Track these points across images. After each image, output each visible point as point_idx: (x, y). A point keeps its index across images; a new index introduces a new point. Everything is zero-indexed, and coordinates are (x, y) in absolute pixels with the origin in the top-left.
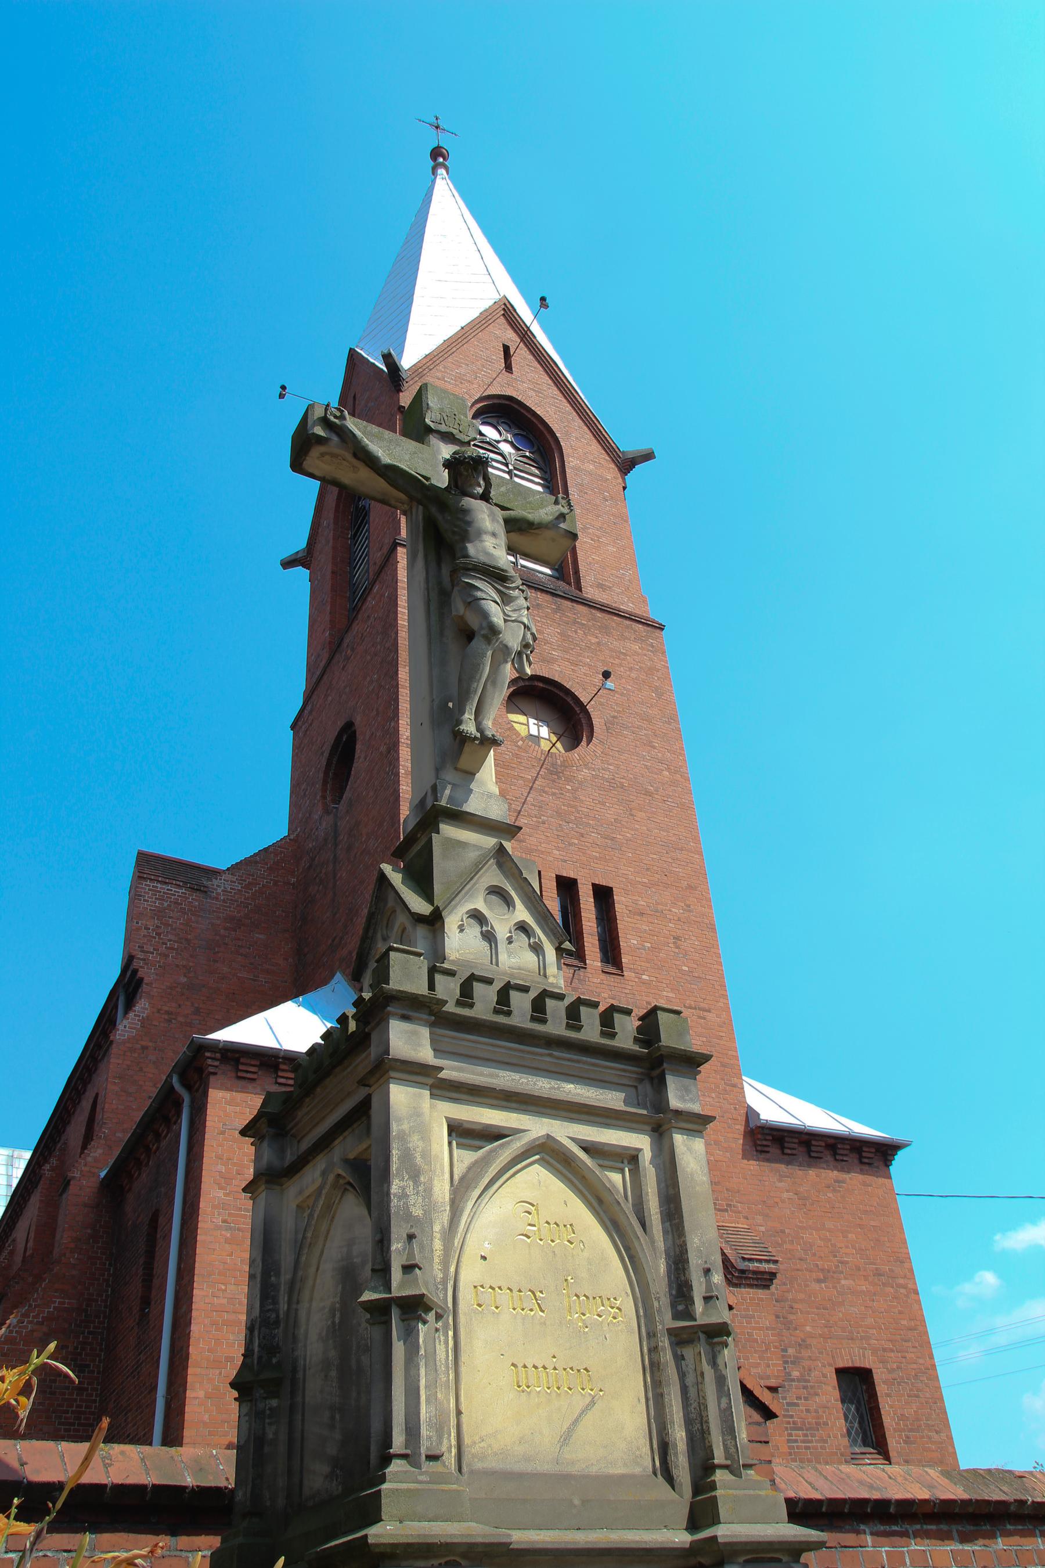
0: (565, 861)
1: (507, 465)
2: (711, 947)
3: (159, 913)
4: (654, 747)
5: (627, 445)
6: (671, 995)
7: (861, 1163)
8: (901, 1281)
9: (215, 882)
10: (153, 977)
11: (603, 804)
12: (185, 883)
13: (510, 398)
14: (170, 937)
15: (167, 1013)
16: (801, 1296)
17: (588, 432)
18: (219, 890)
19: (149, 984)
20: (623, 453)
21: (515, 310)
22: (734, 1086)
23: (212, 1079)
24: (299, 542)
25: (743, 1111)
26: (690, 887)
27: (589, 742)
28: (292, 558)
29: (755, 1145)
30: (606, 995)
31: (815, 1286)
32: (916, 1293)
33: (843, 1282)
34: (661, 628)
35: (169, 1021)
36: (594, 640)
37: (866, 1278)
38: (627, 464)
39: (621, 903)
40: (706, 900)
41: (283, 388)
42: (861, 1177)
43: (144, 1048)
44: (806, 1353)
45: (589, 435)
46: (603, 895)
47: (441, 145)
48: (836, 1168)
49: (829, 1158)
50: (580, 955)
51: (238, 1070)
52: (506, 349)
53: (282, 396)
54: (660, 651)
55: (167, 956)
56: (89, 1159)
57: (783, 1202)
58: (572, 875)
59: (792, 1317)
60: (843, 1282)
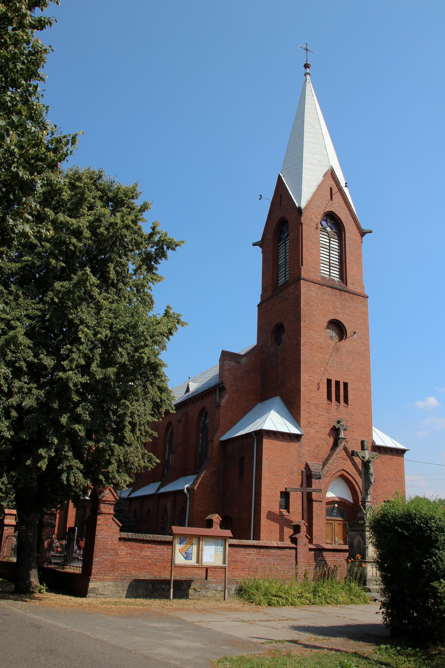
0: (337, 376)
1: (328, 237)
2: (369, 398)
3: (229, 370)
4: (362, 339)
5: (364, 227)
6: (359, 411)
7: (397, 454)
8: (402, 482)
9: (242, 360)
10: (228, 388)
11: (347, 358)
12: (235, 361)
13: (332, 212)
14: (232, 376)
15: (232, 398)
16: (378, 485)
17: (353, 221)
18: (243, 362)
19: (228, 390)
20: (363, 229)
21: (334, 172)
22: (370, 435)
23: (264, 437)
24: (259, 238)
25: (372, 441)
26: (367, 381)
27: (345, 339)
28: (256, 243)
29: (373, 449)
30: (344, 412)
31: (382, 483)
32: (405, 485)
33: (389, 482)
34: (367, 297)
35: (233, 400)
36: (349, 305)
37: (394, 481)
38: (363, 234)
39: (349, 386)
40: (370, 385)
41: (261, 196)
42: (396, 457)
43: (227, 407)
44: (378, 497)
45: (353, 223)
46: (346, 384)
47: (308, 63)
48: (391, 455)
49: (390, 452)
50: (339, 403)
51: (268, 435)
52: (331, 189)
53: (260, 199)
54: (366, 306)
55: (231, 382)
56: (217, 435)
57: (378, 463)
58: (339, 380)
59: (376, 489)
60: (389, 482)
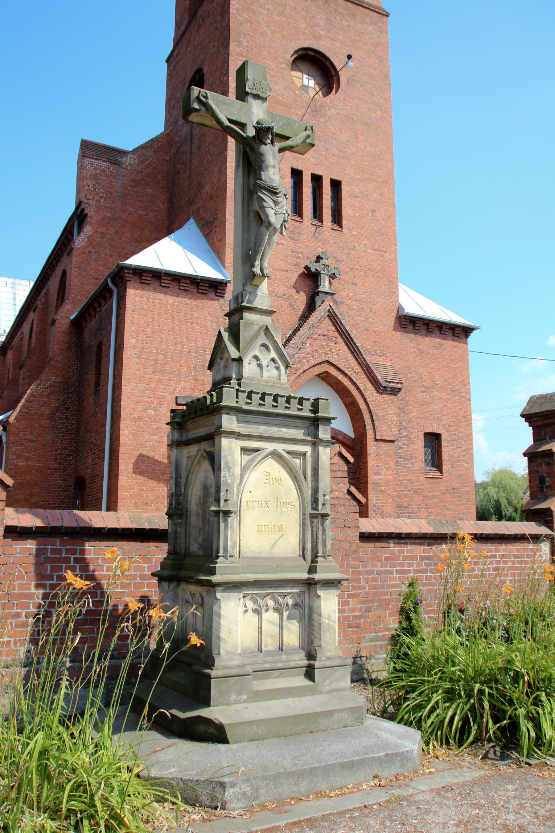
0: (317, 165)
2: (391, 216)
3: (95, 177)
4: (374, 96)
6: (366, 243)
7: (454, 335)
8: (463, 394)
9: (125, 159)
10: (92, 213)
11: (341, 130)
12: (108, 160)
14: (101, 190)
15: (102, 233)
16: (413, 399)
18: (127, 164)
19: (91, 217)
22: (394, 293)
23: (128, 283)
25: (397, 307)
26: (384, 182)
27: (337, 91)
29: (401, 324)
30: (332, 242)
31: (420, 395)
32: (470, 400)
35: (102, 238)
36: (346, 24)
37: (446, 392)
39: (345, 188)
40: (391, 190)
43: (90, 252)
44: (410, 425)
46: (336, 185)
48: (440, 338)
49: (438, 332)
50: (321, 220)
51: (141, 279)
54: (384, 31)
55: (99, 201)
56: (65, 310)
57: (411, 353)
59: (406, 408)
60: (435, 393)
